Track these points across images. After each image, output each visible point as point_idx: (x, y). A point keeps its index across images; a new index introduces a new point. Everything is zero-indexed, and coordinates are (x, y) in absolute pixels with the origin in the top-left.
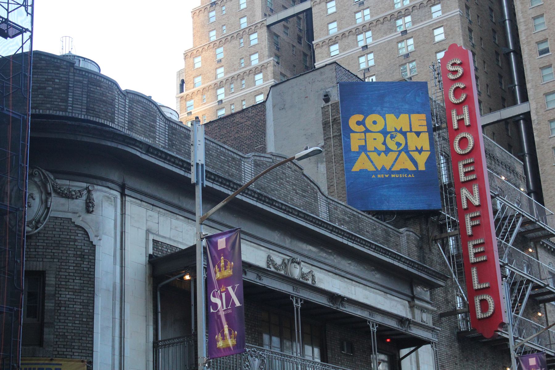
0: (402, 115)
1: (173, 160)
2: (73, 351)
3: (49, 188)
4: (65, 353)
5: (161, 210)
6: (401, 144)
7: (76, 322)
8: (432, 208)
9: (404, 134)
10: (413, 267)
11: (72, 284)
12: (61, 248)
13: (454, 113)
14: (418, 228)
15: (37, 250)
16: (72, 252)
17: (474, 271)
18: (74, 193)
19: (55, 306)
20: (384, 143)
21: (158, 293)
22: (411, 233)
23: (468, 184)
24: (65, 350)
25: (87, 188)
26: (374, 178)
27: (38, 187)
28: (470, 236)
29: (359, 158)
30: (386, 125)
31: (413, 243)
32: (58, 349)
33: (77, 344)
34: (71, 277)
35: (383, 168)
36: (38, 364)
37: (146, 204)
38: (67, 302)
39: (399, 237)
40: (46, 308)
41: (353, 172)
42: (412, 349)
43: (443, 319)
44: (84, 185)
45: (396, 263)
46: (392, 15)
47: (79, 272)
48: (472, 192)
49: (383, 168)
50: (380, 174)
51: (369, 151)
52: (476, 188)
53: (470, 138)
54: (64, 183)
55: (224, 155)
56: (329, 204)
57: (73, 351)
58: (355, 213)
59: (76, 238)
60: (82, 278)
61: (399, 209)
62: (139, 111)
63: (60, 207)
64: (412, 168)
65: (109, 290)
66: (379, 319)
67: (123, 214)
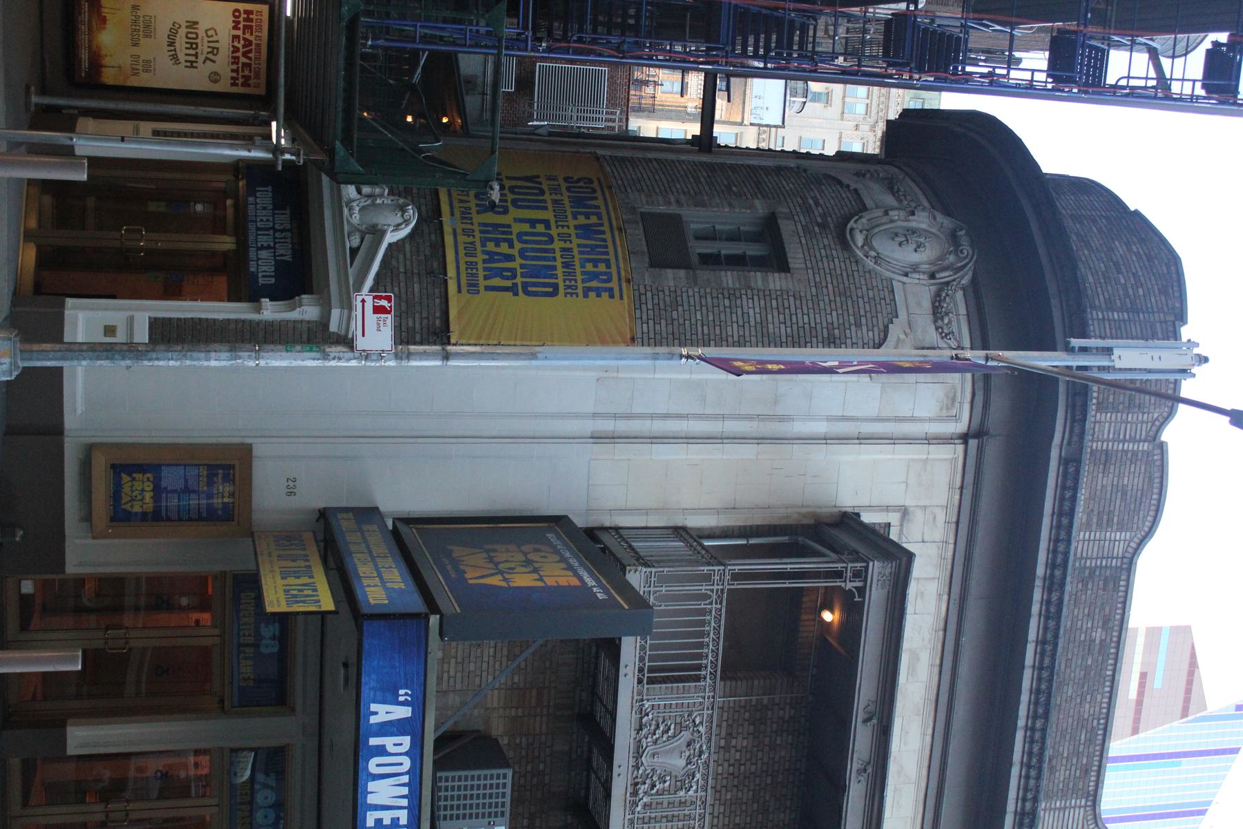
1: (1069, 483)
2: (651, 322)
3: (945, 276)
4: (644, 307)
5: (951, 547)
7: (705, 328)
11: (776, 320)
12: (838, 299)
15: (825, 260)
16: (835, 320)
18: (946, 321)
19: (729, 289)
21: (784, 539)
24: (650, 306)
27: (942, 258)
32: (649, 294)
33: (664, 329)
34: (788, 317)
36: (617, 259)
37: (956, 502)
38: (739, 310)
40: (723, 273)
47: (802, 333)
54: (959, 303)
55: (1090, 741)
57: (651, 322)
59: (864, 328)
60: (790, 339)
62: (1133, 479)
63: (915, 297)
65: (776, 402)
67: (929, 440)
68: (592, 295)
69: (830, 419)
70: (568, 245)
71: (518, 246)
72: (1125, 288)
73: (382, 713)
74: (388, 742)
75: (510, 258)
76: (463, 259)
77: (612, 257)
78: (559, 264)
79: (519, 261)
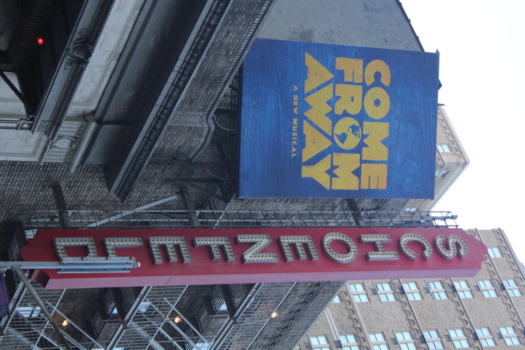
0: (386, 150)
6: (342, 141)
8: (242, 180)
9: (358, 150)
10: (158, 117)
20: (346, 114)
22: (202, 140)
26: (293, 88)
28: (192, 244)
29: (324, 68)
30: (373, 120)
31: (186, 142)
35: (308, 107)
39: (203, 110)
41: (304, 55)
42: (19, 90)
43: (51, 192)
46: (361, 330)
48: (263, 251)
49: (308, 107)
50: (299, 101)
51: (334, 87)
53: (348, 258)
58: (264, 8)
61: (242, 124)
64: (306, 155)
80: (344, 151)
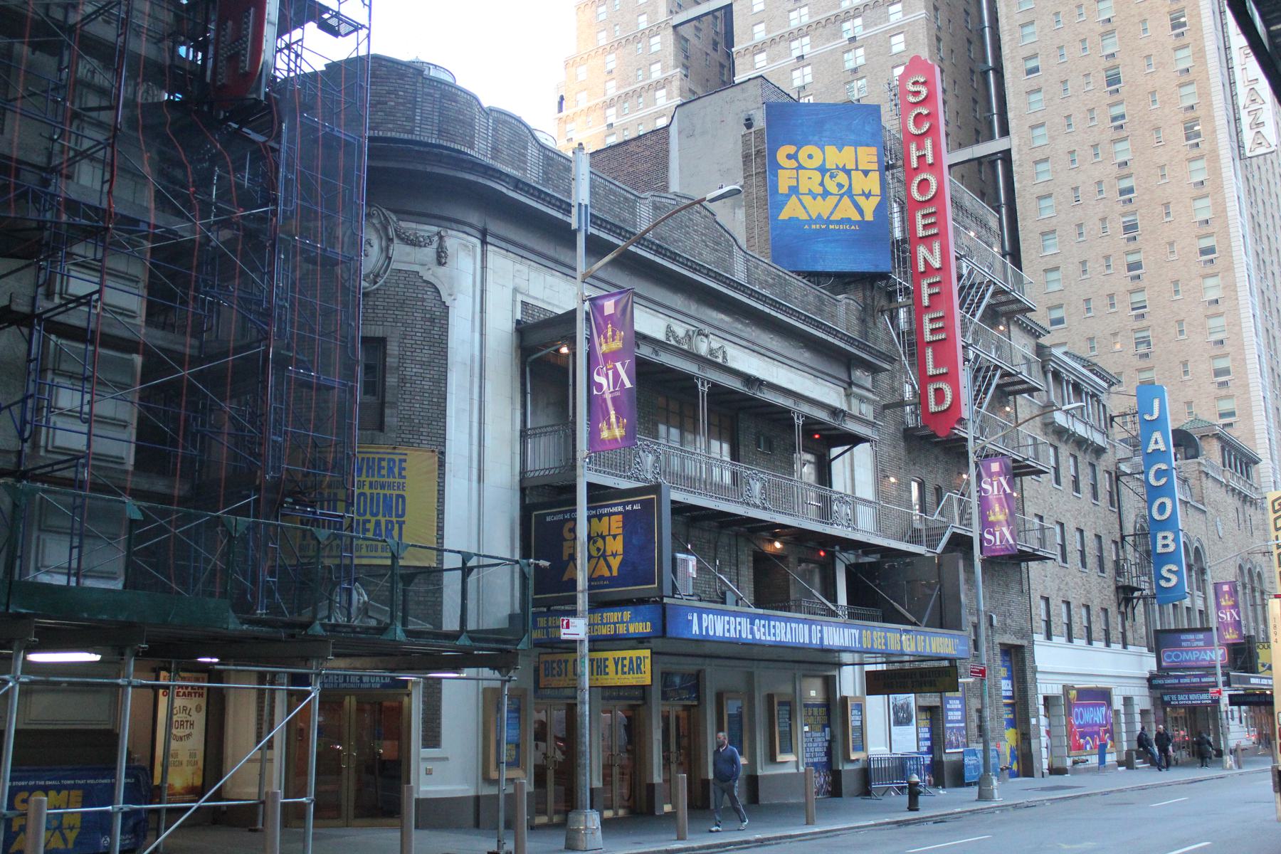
3: (391, 232)
8: (879, 270)
9: (848, 172)
10: (852, 345)
13: (913, 147)
14: (861, 295)
17: (929, 352)
20: (822, 184)
23: (926, 240)
25: (439, 233)
27: (377, 231)
35: (819, 216)
44: (435, 229)
45: (830, 339)
48: (931, 251)
49: (819, 216)
52: (936, 246)
54: (409, 226)
56: (748, 260)
62: (505, 135)
64: (857, 217)
66: (806, 409)
67: (484, 267)
68: (404, 473)
69: (473, 331)
70: (367, 484)
71: (368, 517)
72: (398, 104)
73: (695, 628)
74: (704, 625)
75: (378, 523)
76: (379, 553)
77: (377, 456)
78: (382, 492)
79: (380, 517)
80: (850, 185)
